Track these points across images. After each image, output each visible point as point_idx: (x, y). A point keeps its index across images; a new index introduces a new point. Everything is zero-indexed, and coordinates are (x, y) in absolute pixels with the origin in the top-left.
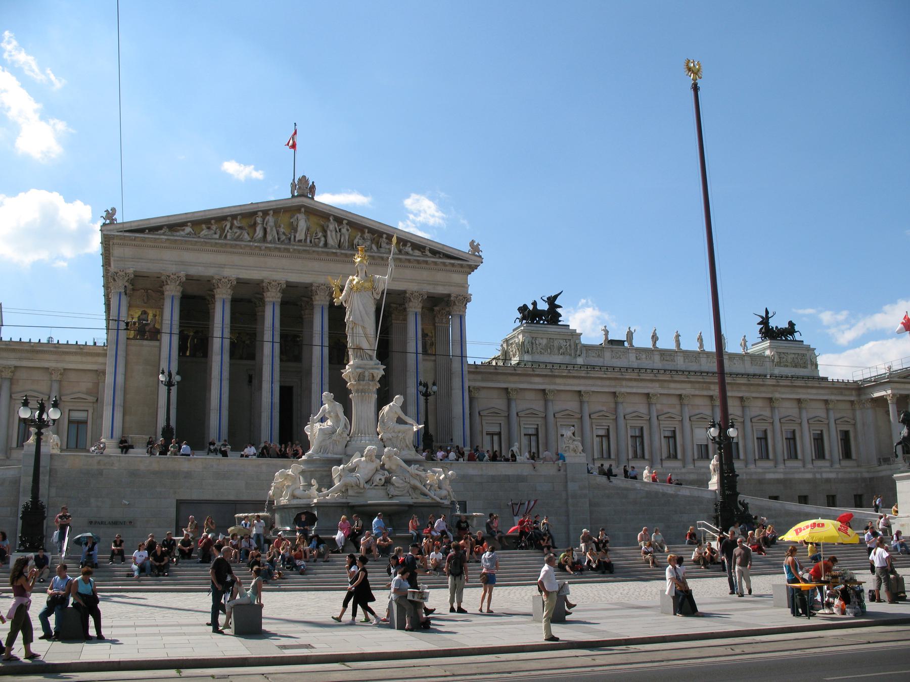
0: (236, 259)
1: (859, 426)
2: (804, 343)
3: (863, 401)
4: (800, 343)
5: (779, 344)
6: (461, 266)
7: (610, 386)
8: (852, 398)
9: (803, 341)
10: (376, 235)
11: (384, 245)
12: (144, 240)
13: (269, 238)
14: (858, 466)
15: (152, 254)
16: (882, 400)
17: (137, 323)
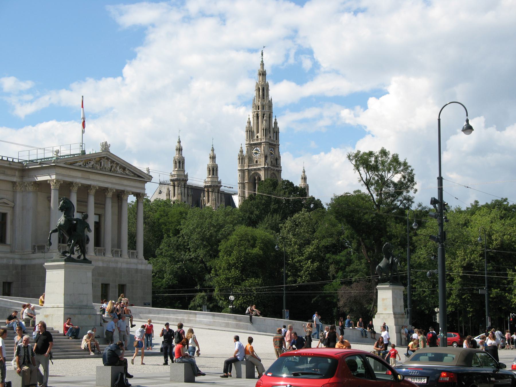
1: (18, 210)
3: (25, 184)
8: (15, 179)
14: (12, 252)
16: (45, 185)
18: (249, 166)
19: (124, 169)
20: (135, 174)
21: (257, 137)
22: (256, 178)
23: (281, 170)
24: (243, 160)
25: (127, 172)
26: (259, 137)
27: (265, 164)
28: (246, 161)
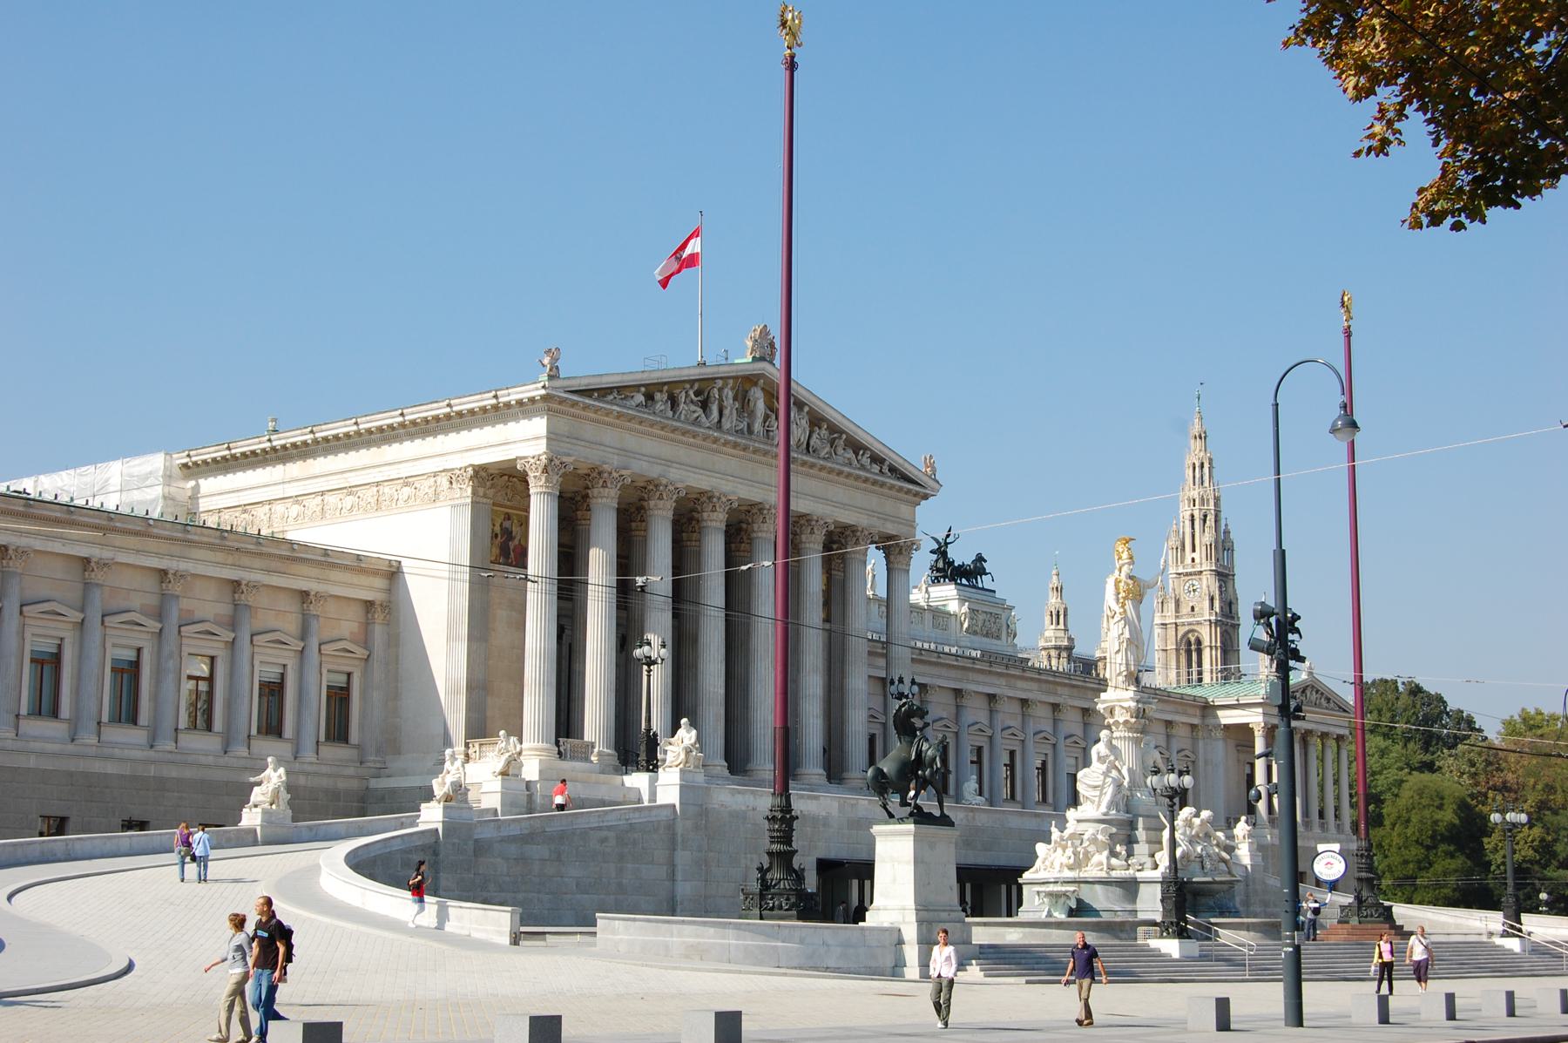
0: (682, 453)
2: (997, 595)
3: (1210, 728)
4: (991, 594)
5: (984, 598)
6: (916, 494)
7: (955, 679)
8: (1196, 721)
9: (994, 592)
10: (836, 435)
11: (840, 451)
12: (586, 407)
13: (726, 424)
15: (589, 431)
16: (1245, 731)
17: (499, 536)
18: (1177, 617)
19: (1328, 700)
20: (1340, 708)
21: (1193, 560)
22: (1193, 639)
23: (1239, 625)
24: (1165, 605)
25: (1332, 705)
26: (1197, 561)
27: (1210, 614)
28: (1172, 606)
